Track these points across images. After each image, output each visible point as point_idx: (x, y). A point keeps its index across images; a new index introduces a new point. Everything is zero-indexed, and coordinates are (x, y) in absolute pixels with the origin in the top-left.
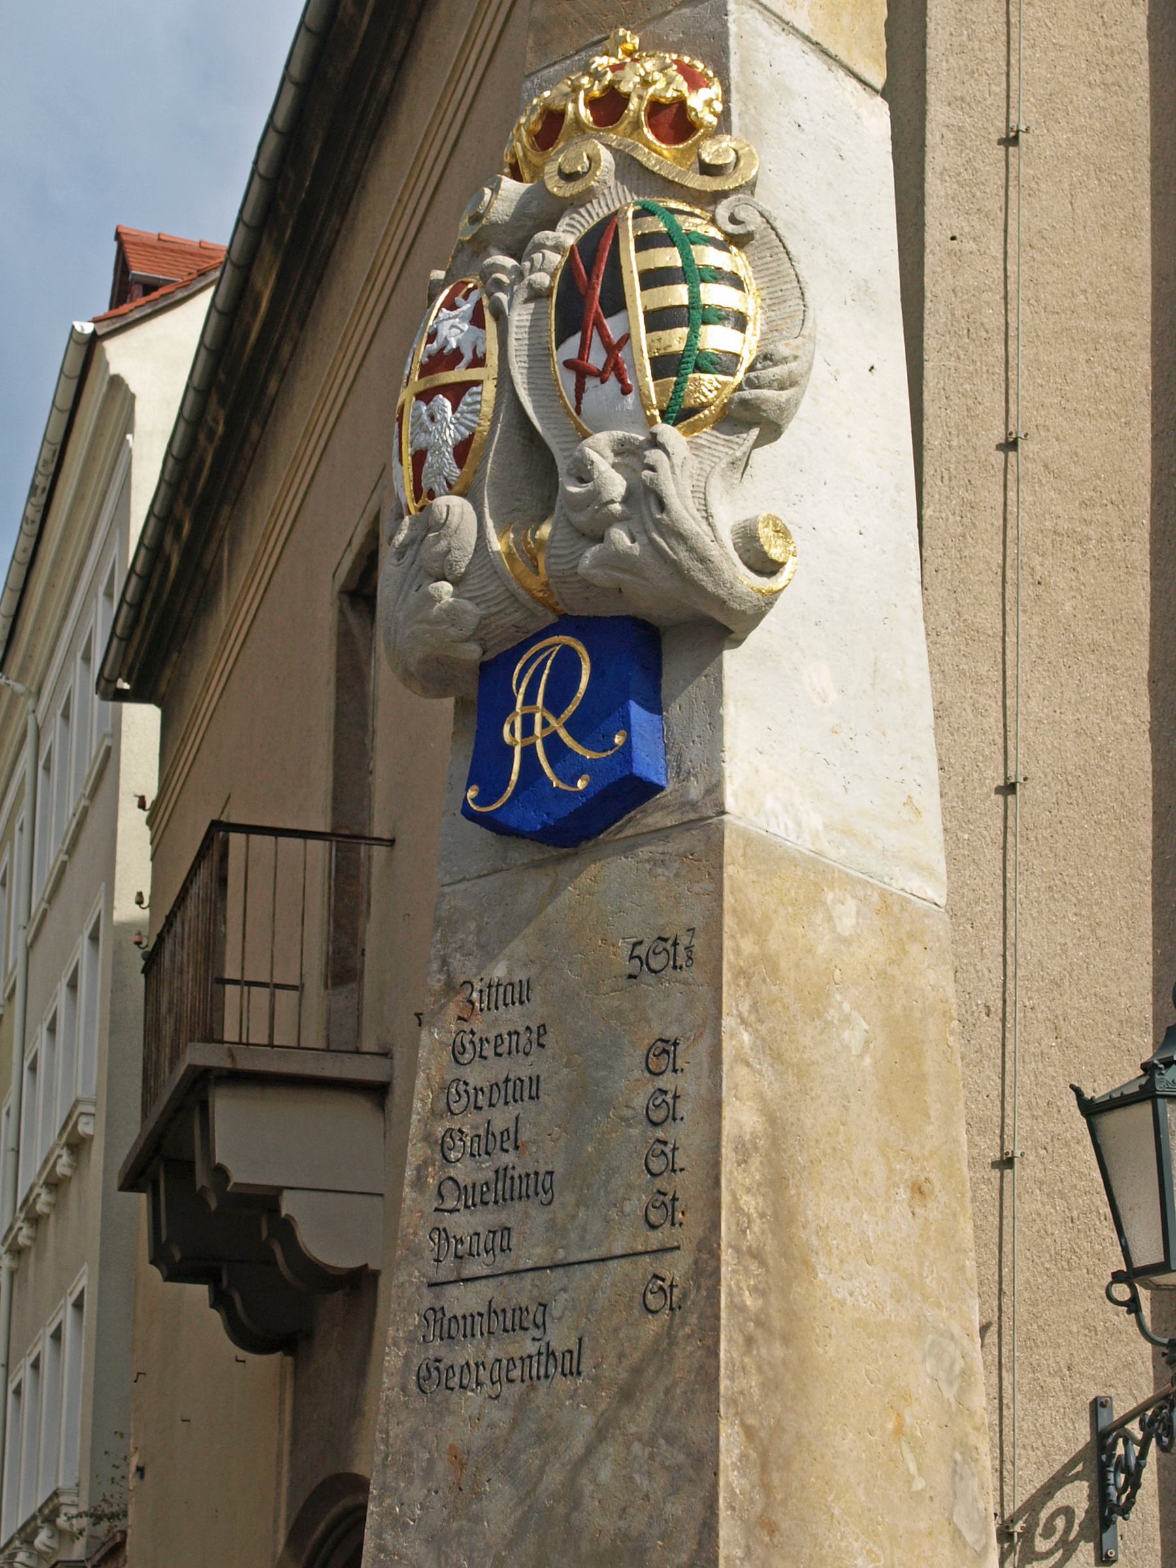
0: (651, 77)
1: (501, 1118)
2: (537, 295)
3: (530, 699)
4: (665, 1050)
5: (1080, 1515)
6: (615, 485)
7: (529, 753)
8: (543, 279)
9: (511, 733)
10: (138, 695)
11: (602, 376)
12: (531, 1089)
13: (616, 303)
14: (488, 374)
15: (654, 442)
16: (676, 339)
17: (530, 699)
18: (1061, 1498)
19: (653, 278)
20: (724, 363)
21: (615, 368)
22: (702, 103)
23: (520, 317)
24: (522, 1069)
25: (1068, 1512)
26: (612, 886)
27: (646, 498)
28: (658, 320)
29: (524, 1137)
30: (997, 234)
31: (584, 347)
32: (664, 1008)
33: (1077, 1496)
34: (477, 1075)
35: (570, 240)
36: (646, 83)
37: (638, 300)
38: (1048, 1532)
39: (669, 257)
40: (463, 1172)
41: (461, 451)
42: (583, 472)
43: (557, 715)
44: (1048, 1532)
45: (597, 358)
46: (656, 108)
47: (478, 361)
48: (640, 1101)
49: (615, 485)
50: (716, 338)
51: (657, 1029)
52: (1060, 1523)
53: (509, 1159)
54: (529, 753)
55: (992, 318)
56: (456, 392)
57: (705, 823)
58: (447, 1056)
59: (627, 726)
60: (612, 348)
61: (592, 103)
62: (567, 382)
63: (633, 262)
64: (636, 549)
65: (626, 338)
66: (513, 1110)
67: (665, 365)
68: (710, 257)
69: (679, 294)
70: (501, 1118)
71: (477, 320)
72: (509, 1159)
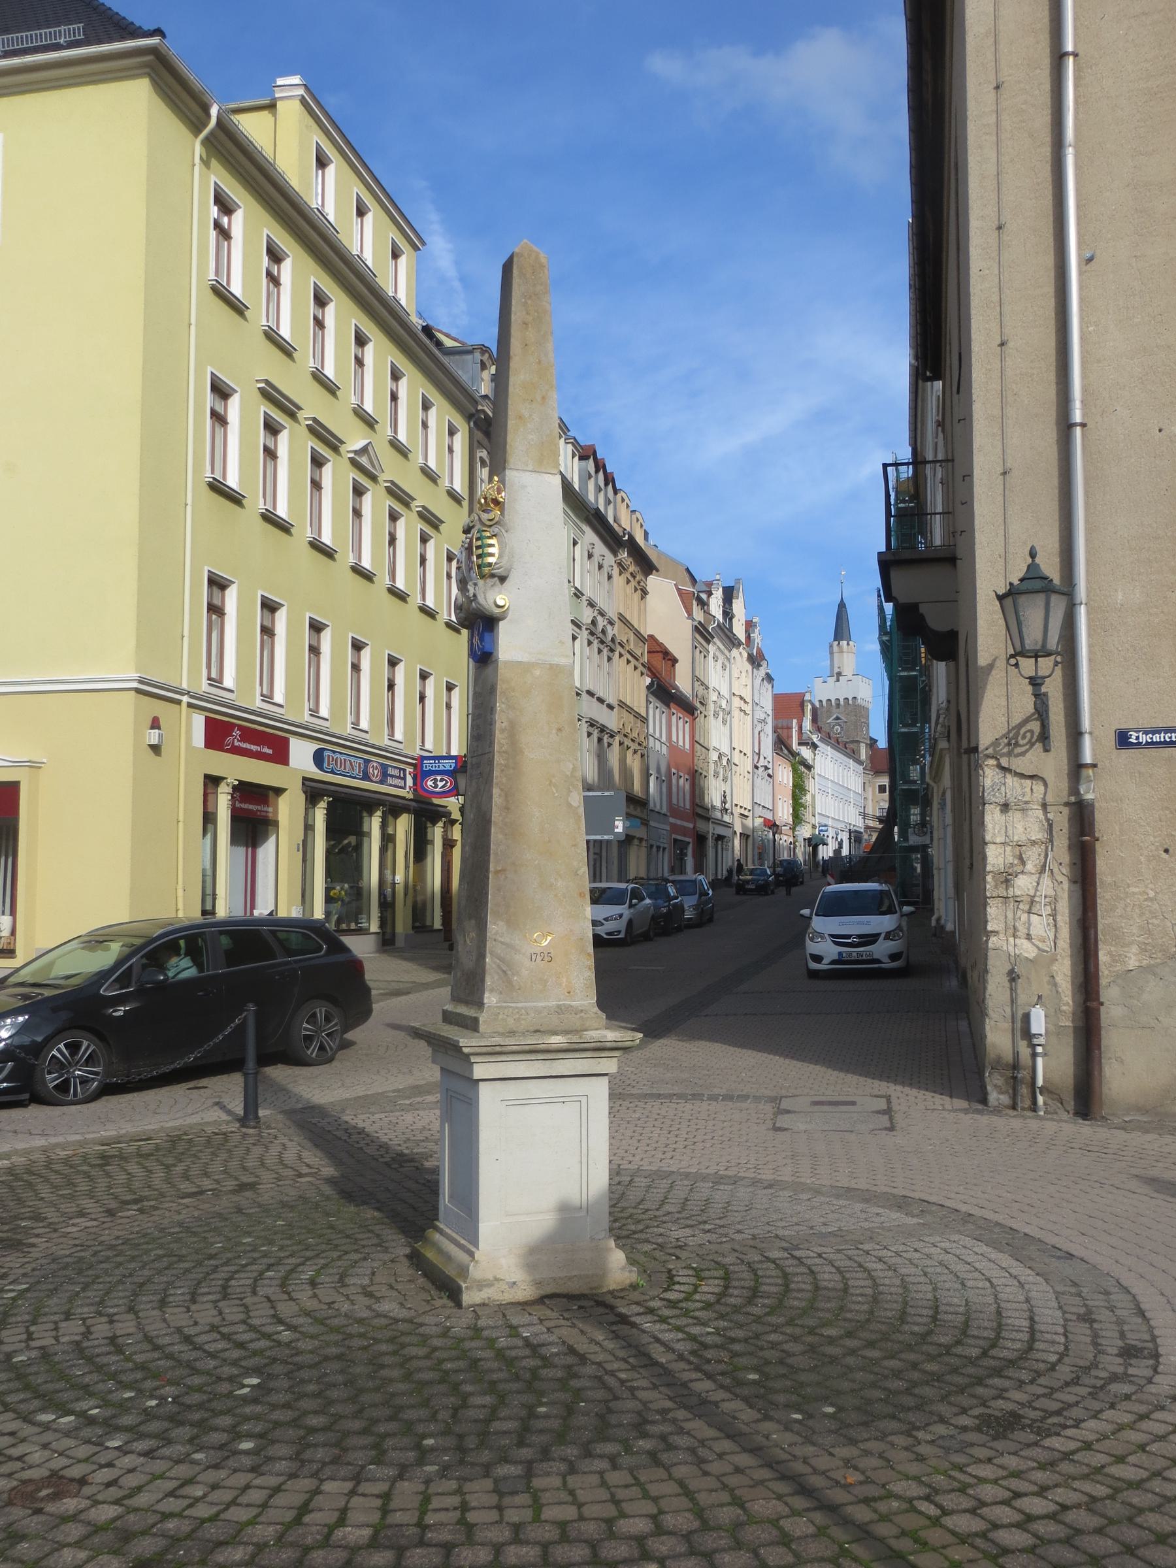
5: (1037, 734)
10: (932, 379)
18: (1029, 726)
19: (478, 547)
20: (490, 564)
25: (1032, 732)
28: (479, 557)
30: (996, 265)
33: (1035, 726)
37: (476, 552)
44: (1024, 737)
52: (1028, 735)
55: (995, 298)
57: (497, 661)
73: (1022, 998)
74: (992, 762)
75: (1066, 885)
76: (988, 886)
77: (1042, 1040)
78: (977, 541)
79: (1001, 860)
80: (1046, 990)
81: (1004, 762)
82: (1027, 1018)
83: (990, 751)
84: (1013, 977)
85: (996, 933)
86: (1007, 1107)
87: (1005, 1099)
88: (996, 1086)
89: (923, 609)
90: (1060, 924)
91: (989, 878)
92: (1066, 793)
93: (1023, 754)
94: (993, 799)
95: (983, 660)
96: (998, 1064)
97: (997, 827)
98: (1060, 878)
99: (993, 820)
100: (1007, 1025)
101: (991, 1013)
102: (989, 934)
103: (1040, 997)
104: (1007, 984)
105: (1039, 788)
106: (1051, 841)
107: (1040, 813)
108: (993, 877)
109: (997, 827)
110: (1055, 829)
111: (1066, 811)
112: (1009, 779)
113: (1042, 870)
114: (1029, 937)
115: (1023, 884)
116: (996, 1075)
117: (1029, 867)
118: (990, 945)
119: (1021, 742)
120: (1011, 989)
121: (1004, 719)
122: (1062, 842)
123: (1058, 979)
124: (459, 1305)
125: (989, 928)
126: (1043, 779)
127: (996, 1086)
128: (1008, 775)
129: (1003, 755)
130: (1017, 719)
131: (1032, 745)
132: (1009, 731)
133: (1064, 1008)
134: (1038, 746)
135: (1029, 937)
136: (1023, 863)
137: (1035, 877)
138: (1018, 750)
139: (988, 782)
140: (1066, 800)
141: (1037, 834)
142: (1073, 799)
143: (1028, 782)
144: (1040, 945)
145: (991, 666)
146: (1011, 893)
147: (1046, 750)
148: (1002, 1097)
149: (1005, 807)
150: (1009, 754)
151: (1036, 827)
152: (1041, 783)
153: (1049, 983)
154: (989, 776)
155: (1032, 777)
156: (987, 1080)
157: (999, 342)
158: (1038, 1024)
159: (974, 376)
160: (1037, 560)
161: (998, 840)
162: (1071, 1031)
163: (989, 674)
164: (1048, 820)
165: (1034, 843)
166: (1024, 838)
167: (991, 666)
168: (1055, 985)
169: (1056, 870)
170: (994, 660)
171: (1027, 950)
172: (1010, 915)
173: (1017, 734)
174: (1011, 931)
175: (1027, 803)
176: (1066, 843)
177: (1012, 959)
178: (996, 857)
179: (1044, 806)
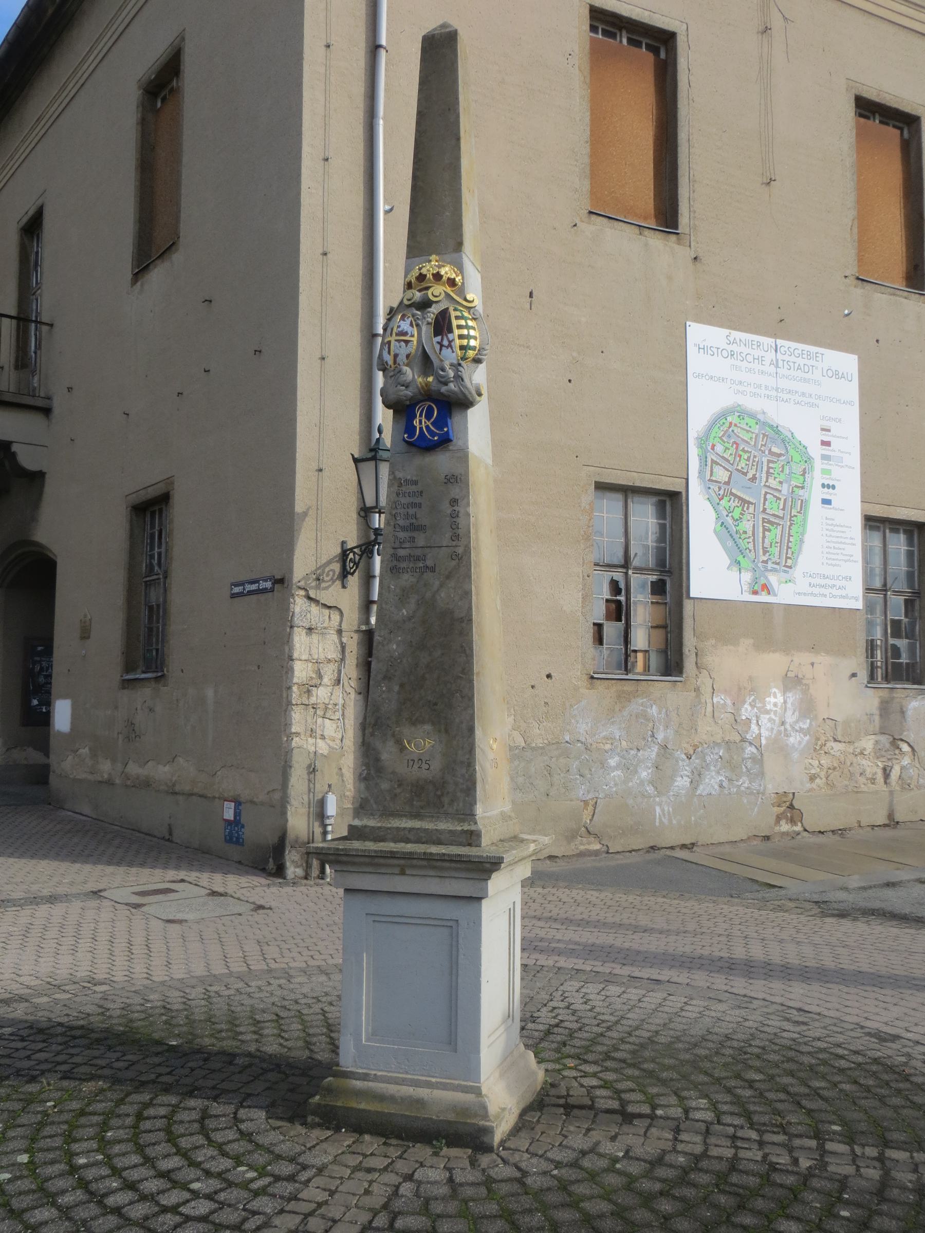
0: (447, 271)
1: (411, 511)
2: (429, 323)
3: (421, 415)
4: (454, 502)
5: (337, 573)
6: (451, 374)
7: (421, 429)
8: (430, 320)
9: (416, 423)
11: (447, 347)
12: (420, 506)
13: (450, 330)
14: (415, 339)
15: (460, 365)
16: (465, 342)
17: (421, 415)
19: (459, 327)
20: (474, 348)
21: (450, 345)
22: (458, 279)
23: (424, 328)
24: (417, 500)
25: (334, 571)
26: (441, 461)
27: (459, 378)
28: (461, 337)
29: (418, 516)
31: (442, 339)
32: (455, 492)
33: (337, 567)
34: (404, 500)
35: (436, 312)
36: (446, 273)
37: (457, 332)
38: (328, 575)
39: (463, 322)
40: (401, 522)
41: (408, 356)
42: (443, 370)
43: (429, 420)
44: (328, 575)
45: (445, 343)
46: (449, 279)
47: (412, 336)
48: (449, 512)
49: (451, 374)
50: (473, 343)
51: (453, 496)
52: (331, 573)
53: (414, 521)
54: (421, 429)
56: (407, 342)
58: (395, 495)
59: (447, 426)
60: (450, 342)
61: (433, 275)
62: (437, 347)
63: (455, 323)
64: (456, 389)
65: (453, 340)
66: (414, 510)
67: (462, 348)
68: (470, 323)
69: (465, 332)
70: (411, 511)
71: (411, 325)
72: (414, 521)
73: (320, 787)
74: (302, 593)
75: (353, 695)
76: (294, 695)
77: (331, 821)
78: (299, 408)
79: (304, 673)
80: (334, 780)
81: (312, 594)
82: (322, 803)
83: (302, 584)
84: (312, 770)
85: (297, 734)
86: (301, 878)
87: (300, 872)
88: (293, 861)
89: (15, 448)
90: (347, 726)
91: (295, 688)
92: (356, 623)
93: (327, 588)
94: (301, 624)
95: (299, 508)
96: (296, 844)
97: (303, 647)
98: (349, 690)
99: (300, 642)
100: (304, 810)
101: (293, 802)
102: (290, 736)
103: (330, 786)
104: (306, 777)
105: (336, 617)
106: (343, 659)
107: (335, 637)
108: (298, 688)
109: (303, 647)
110: (348, 650)
111: (356, 636)
112: (314, 609)
113: (338, 681)
114: (323, 737)
115: (322, 694)
116: (294, 852)
117: (326, 680)
118: (294, 744)
119: (326, 579)
120: (309, 780)
121: (314, 558)
122: (352, 660)
123: (344, 770)
124: (488, 1149)
125: (293, 730)
126: (339, 610)
127: (293, 861)
128: (313, 605)
129: (312, 588)
130: (324, 560)
131: (334, 582)
132: (318, 569)
133: (348, 793)
134: (338, 583)
135: (323, 737)
136: (320, 677)
137: (330, 689)
138: (323, 585)
139: (297, 610)
140: (356, 628)
141: (334, 654)
142: (364, 628)
143: (326, 611)
144: (331, 743)
145: (305, 514)
146: (313, 700)
147: (344, 587)
148: (297, 870)
149: (310, 630)
150: (318, 587)
151: (332, 648)
152: (337, 613)
153: (337, 774)
154: (299, 605)
155: (329, 607)
156: (287, 857)
157: (321, 251)
158: (331, 809)
159: (301, 272)
160: (383, 435)
161: (304, 657)
162: (351, 812)
163: (303, 520)
164: (342, 643)
165: (329, 661)
166: (322, 656)
167: (305, 514)
168: (342, 775)
169: (346, 684)
170: (308, 509)
171: (323, 747)
172: (309, 720)
173: (323, 572)
174: (309, 732)
175: (325, 628)
176: (354, 662)
177: (312, 755)
178: (301, 671)
179: (340, 632)
